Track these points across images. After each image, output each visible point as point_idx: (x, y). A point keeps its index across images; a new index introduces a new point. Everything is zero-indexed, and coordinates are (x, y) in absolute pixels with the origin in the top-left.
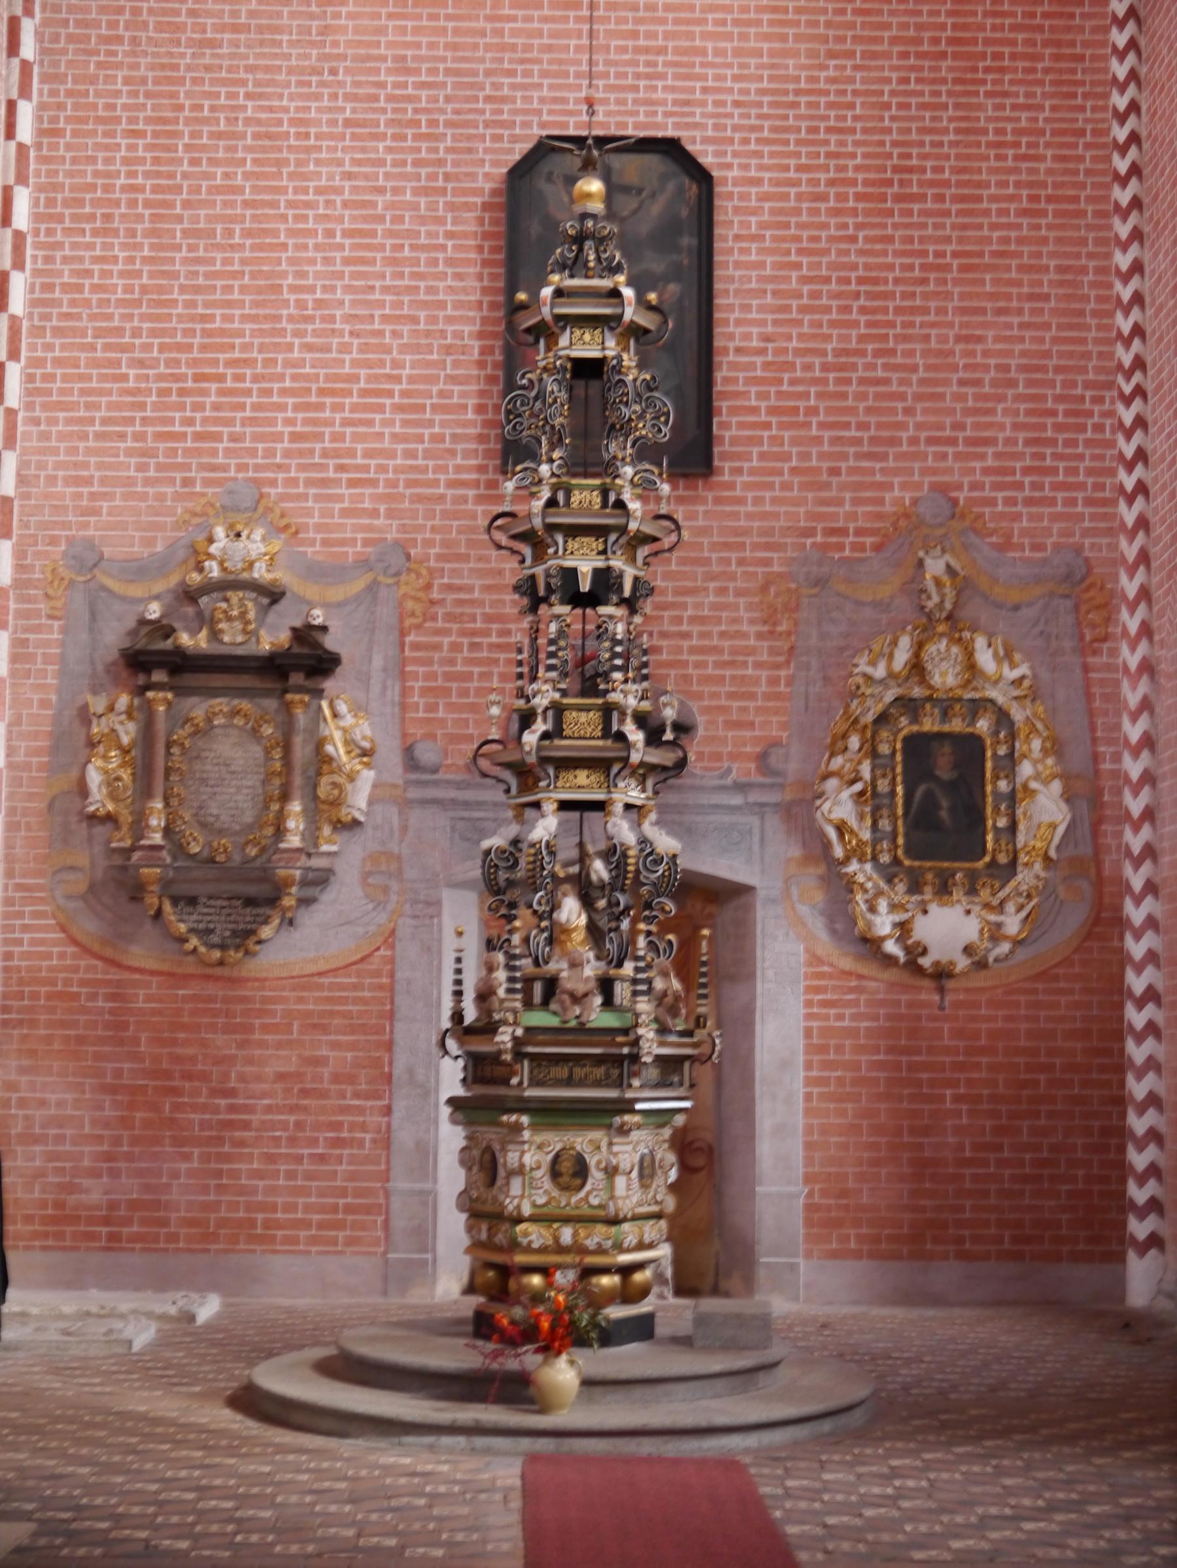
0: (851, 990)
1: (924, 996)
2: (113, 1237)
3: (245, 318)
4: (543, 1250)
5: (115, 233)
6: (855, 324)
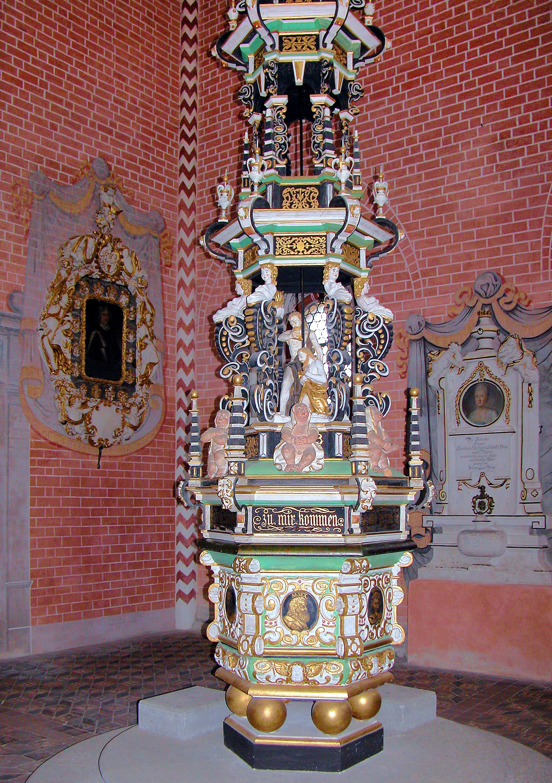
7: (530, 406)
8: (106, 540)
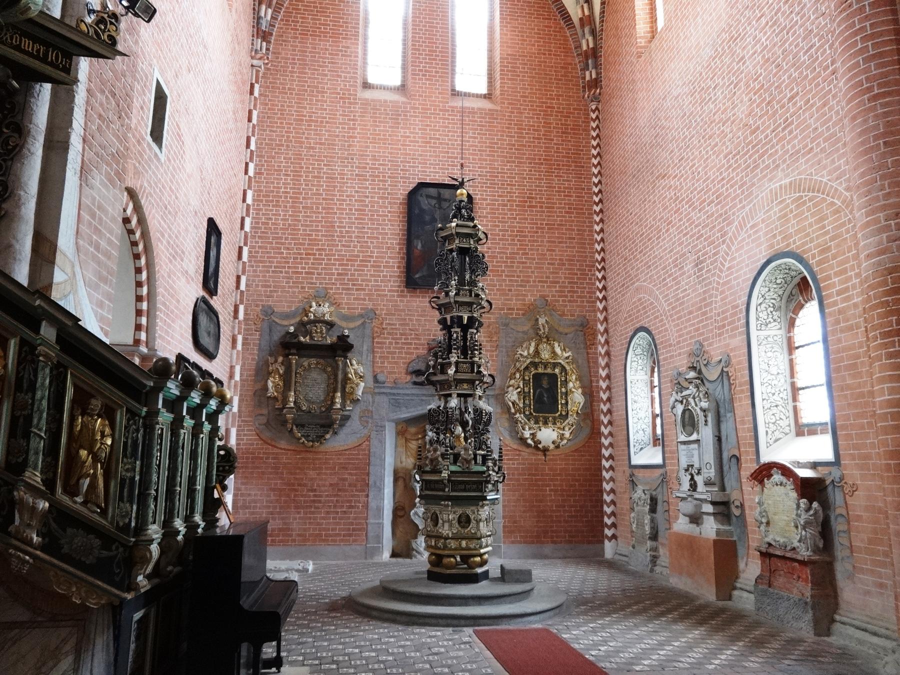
1: (539, 457)
3: (322, 236)
5: (280, 206)
6: (516, 245)
7: (706, 425)
8: (551, 501)
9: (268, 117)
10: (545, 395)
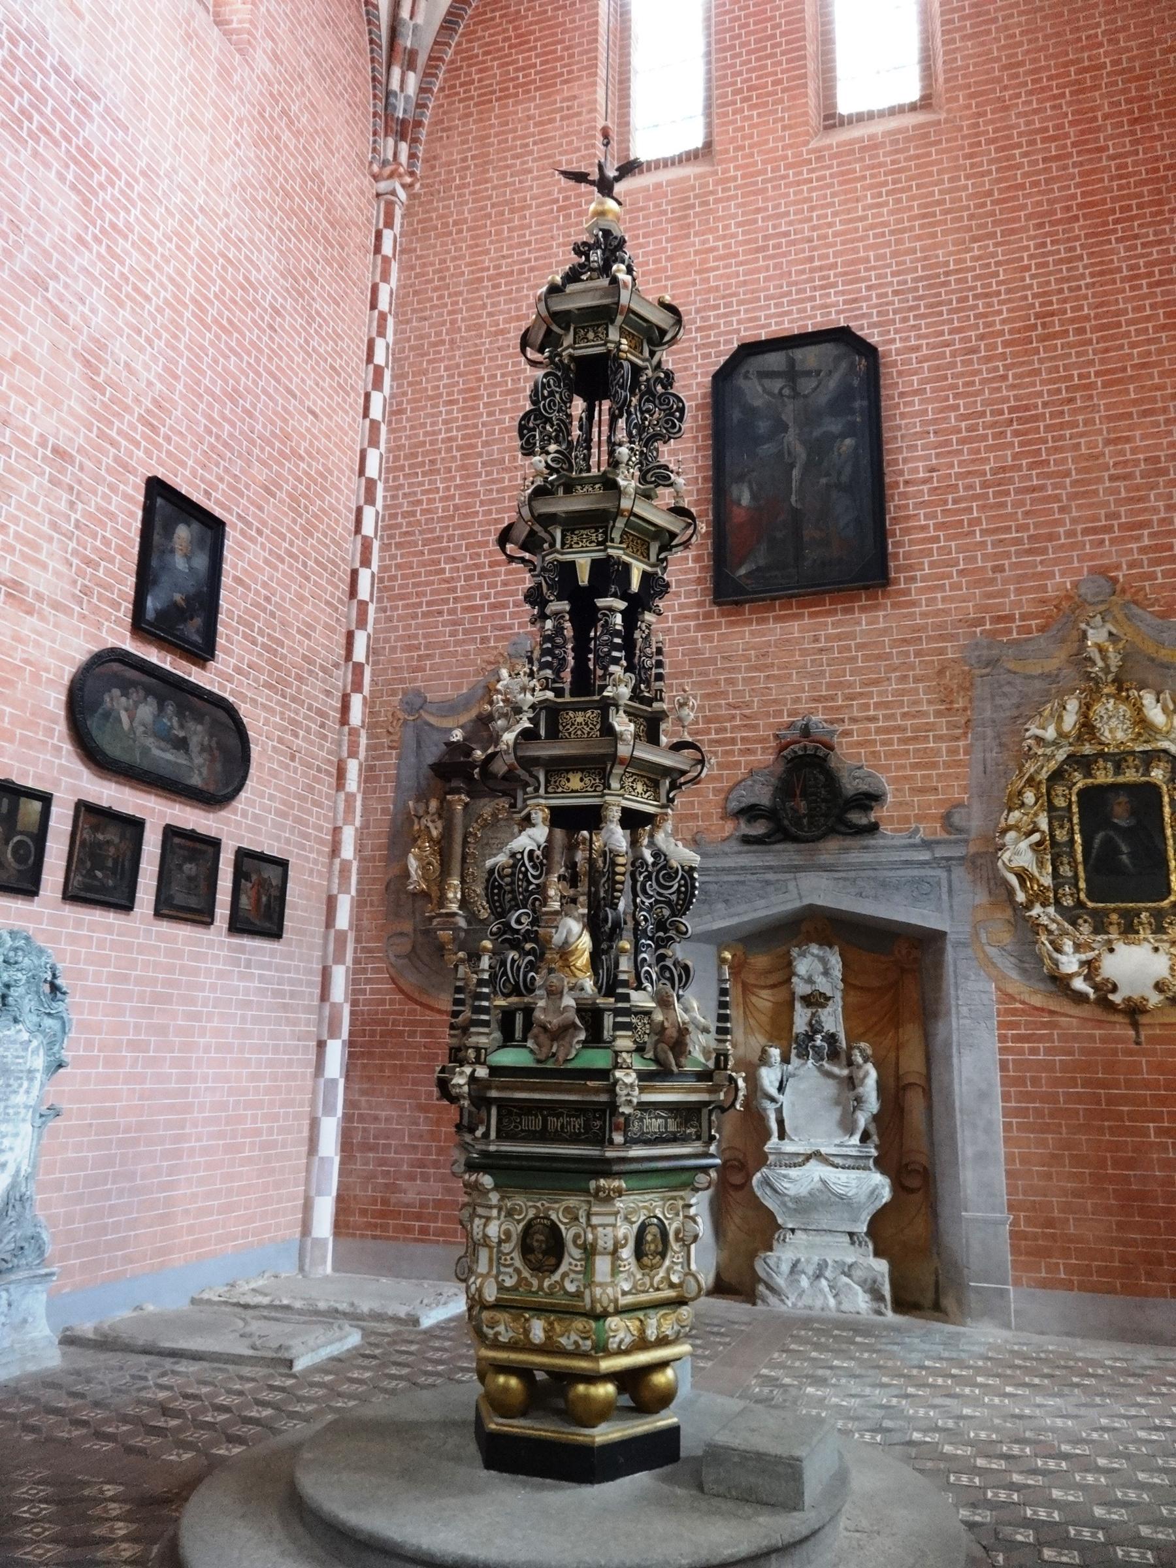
0: (1044, 1025)
2: (424, 1231)
4: (512, 1346)
5: (438, 471)
9: (416, 293)
10: (1125, 849)
